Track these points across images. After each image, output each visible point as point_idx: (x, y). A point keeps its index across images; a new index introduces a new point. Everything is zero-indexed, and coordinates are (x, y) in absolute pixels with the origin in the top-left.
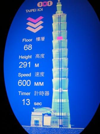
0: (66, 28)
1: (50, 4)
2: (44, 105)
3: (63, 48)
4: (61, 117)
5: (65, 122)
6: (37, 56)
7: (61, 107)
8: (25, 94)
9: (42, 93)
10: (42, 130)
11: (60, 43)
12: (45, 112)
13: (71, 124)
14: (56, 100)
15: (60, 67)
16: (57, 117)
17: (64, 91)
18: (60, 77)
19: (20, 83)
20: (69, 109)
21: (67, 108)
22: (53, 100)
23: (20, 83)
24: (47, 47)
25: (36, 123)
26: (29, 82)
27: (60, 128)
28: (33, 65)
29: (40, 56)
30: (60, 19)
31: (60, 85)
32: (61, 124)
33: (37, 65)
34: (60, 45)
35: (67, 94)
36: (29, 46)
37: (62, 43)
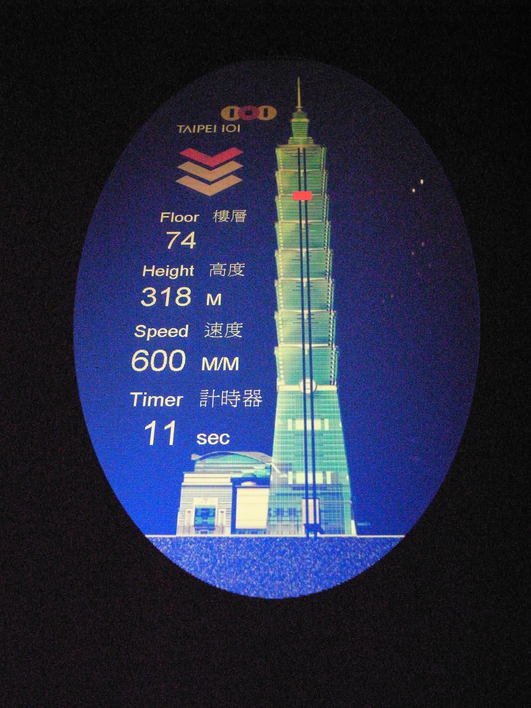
0: (324, 187)
1: (266, 115)
2: (238, 445)
3: (312, 247)
4: (310, 492)
5: (331, 511)
7: (310, 450)
8: (159, 400)
9: (230, 398)
10: (228, 550)
11: (304, 231)
12: (246, 473)
13: (357, 517)
14: (290, 421)
15: (306, 306)
16: (296, 492)
17: (321, 388)
19: (140, 361)
21: (336, 453)
22: (278, 422)
23: (140, 361)
24: (258, 243)
25: (200, 521)
26: (178, 357)
27: (308, 538)
28: (198, 298)
29: (227, 272)
31: (307, 368)
32: (311, 521)
33: (213, 300)
35: (335, 399)
36: (178, 292)
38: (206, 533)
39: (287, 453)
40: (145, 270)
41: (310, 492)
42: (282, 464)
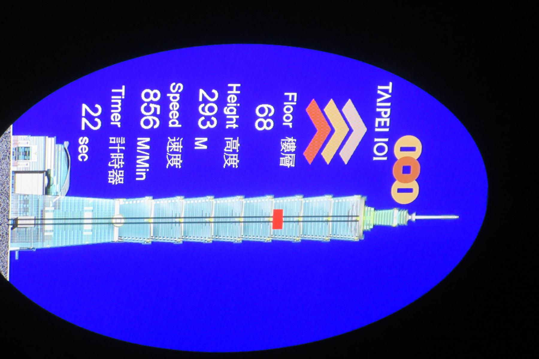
6: (232, 144)
17: (116, 230)
30: (342, 219)
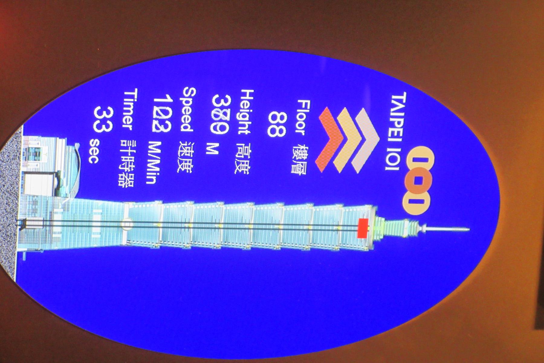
4: (48, 223)
14: (101, 211)
17: (125, 233)
18: (166, 225)
20: (72, 247)
25: (32, 151)
31: (140, 224)
32: (27, 223)
34: (264, 227)
37: (271, 232)
38: (24, 155)
39: (76, 208)
40: (248, 91)
41: (48, 223)
42: (68, 205)
